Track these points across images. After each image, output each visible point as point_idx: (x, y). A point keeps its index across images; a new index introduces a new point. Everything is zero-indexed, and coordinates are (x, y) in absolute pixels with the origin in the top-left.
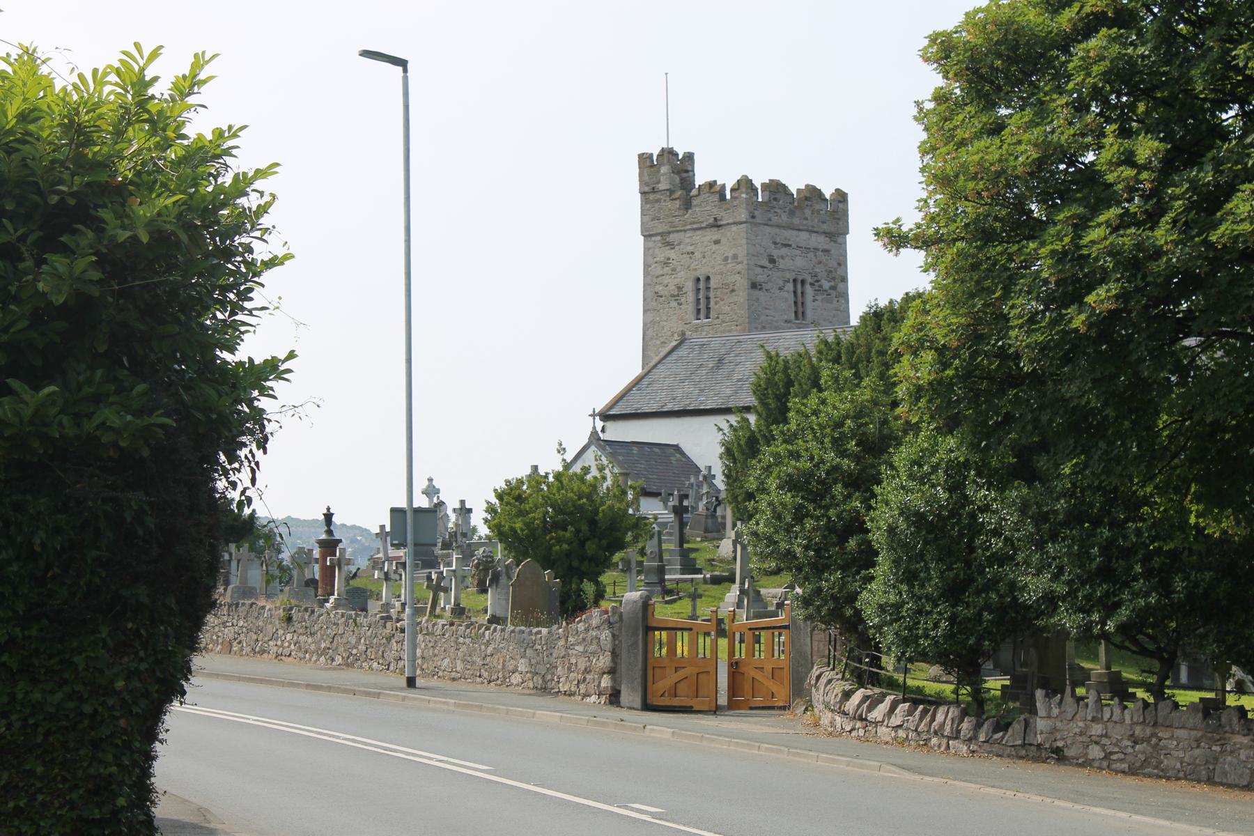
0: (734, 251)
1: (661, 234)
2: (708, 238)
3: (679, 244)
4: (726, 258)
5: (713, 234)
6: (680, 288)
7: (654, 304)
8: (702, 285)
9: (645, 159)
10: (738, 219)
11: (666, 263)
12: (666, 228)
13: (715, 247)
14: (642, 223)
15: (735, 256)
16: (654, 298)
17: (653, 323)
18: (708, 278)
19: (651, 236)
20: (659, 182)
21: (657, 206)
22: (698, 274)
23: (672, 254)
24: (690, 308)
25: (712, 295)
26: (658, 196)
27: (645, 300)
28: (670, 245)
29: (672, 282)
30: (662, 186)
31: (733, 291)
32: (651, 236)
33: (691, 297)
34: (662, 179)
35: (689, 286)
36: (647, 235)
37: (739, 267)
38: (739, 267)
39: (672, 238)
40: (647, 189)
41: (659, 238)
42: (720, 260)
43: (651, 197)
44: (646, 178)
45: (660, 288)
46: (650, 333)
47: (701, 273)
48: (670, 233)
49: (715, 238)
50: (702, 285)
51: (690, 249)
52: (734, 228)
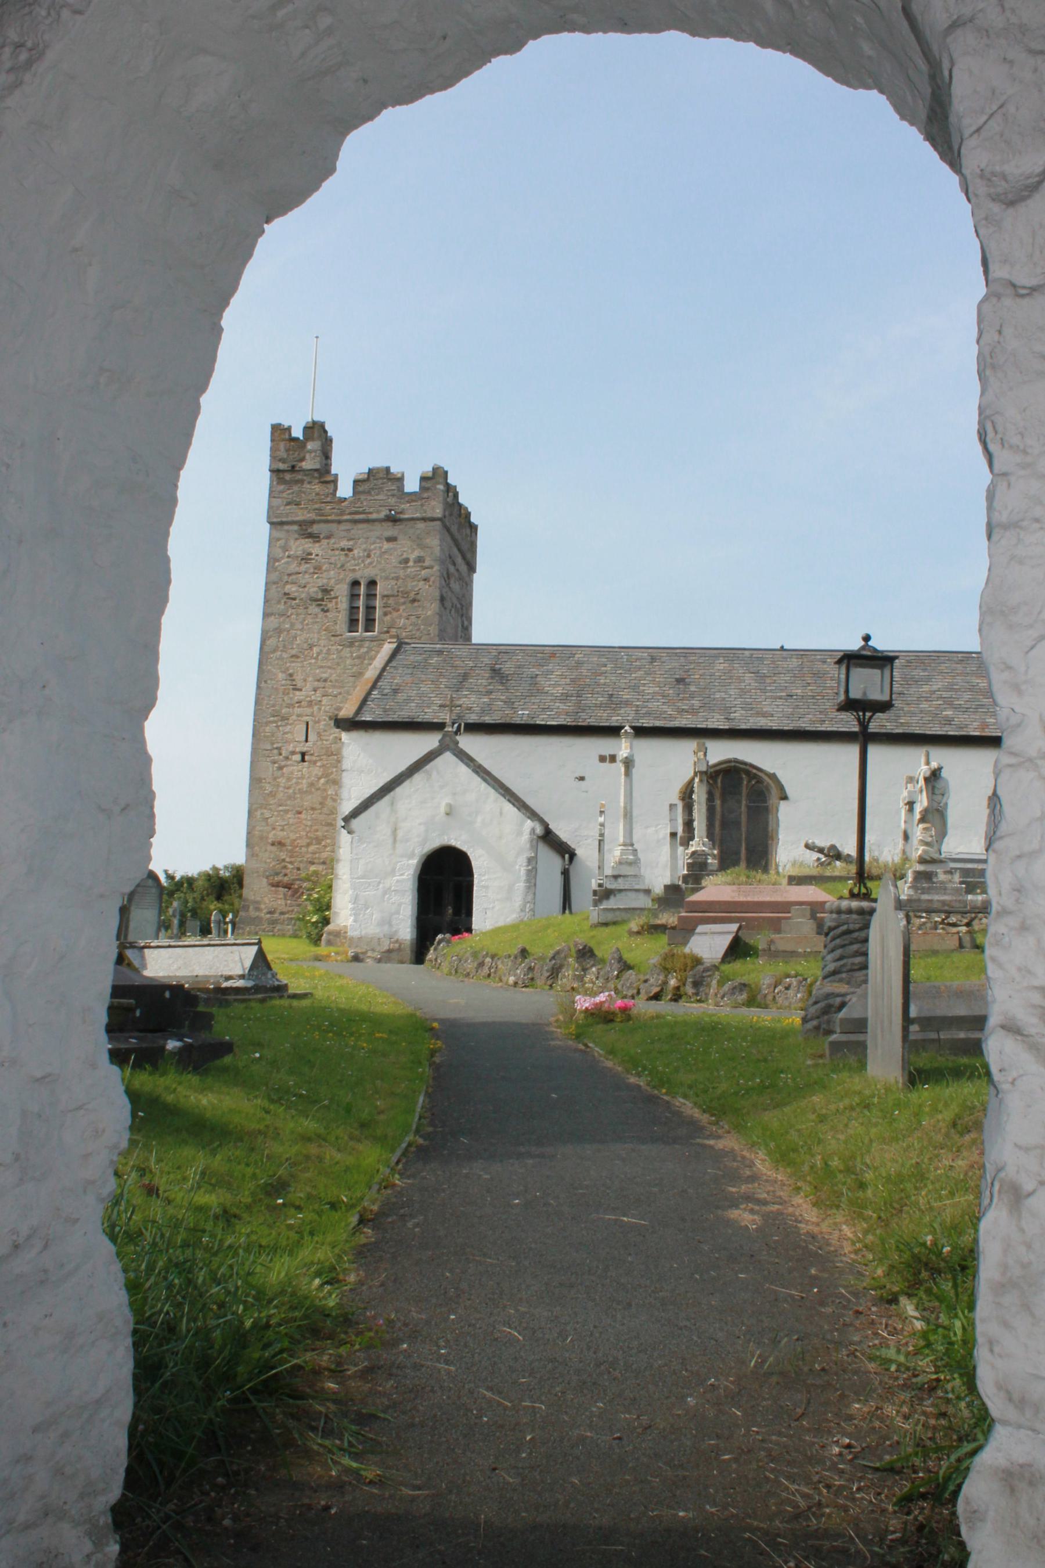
0: (416, 553)
1: (300, 523)
2: (378, 534)
3: (328, 537)
4: (407, 561)
5: (390, 530)
6: (326, 591)
7: (282, 607)
8: (362, 590)
9: (279, 432)
10: (429, 515)
11: (306, 558)
12: (312, 516)
13: (386, 546)
14: (270, 507)
15: (420, 560)
16: (280, 599)
17: (279, 631)
18: (372, 583)
19: (282, 523)
20: (303, 459)
21: (296, 488)
22: (357, 575)
23: (316, 549)
24: (343, 617)
25: (378, 603)
26: (299, 477)
27: (266, 601)
28: (315, 537)
29: (313, 585)
30: (306, 465)
31: (414, 601)
32: (282, 523)
33: (344, 604)
34: (308, 456)
35: (342, 591)
36: (276, 523)
37: (424, 573)
38: (424, 573)
39: (315, 529)
40: (282, 466)
41: (296, 527)
42: (394, 560)
43: (288, 477)
44: (282, 454)
45: (291, 588)
46: (272, 642)
47: (363, 574)
48: (313, 522)
49: (389, 533)
50: (362, 590)
51: (345, 544)
52: (421, 525)
